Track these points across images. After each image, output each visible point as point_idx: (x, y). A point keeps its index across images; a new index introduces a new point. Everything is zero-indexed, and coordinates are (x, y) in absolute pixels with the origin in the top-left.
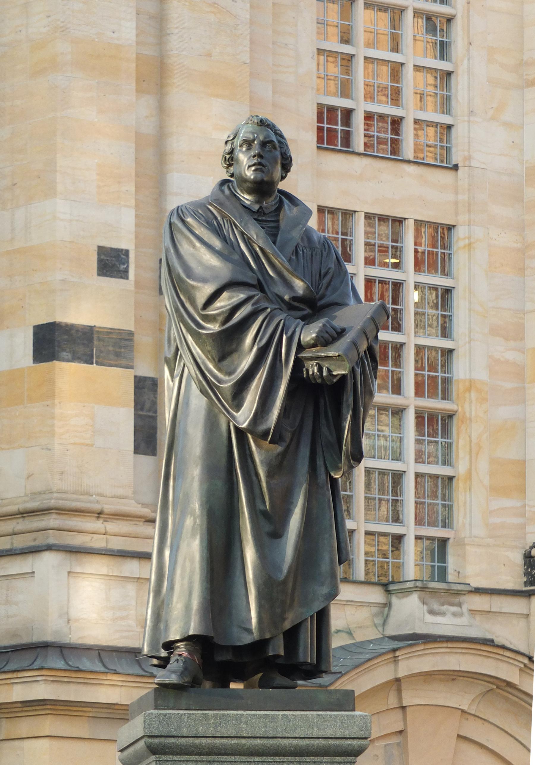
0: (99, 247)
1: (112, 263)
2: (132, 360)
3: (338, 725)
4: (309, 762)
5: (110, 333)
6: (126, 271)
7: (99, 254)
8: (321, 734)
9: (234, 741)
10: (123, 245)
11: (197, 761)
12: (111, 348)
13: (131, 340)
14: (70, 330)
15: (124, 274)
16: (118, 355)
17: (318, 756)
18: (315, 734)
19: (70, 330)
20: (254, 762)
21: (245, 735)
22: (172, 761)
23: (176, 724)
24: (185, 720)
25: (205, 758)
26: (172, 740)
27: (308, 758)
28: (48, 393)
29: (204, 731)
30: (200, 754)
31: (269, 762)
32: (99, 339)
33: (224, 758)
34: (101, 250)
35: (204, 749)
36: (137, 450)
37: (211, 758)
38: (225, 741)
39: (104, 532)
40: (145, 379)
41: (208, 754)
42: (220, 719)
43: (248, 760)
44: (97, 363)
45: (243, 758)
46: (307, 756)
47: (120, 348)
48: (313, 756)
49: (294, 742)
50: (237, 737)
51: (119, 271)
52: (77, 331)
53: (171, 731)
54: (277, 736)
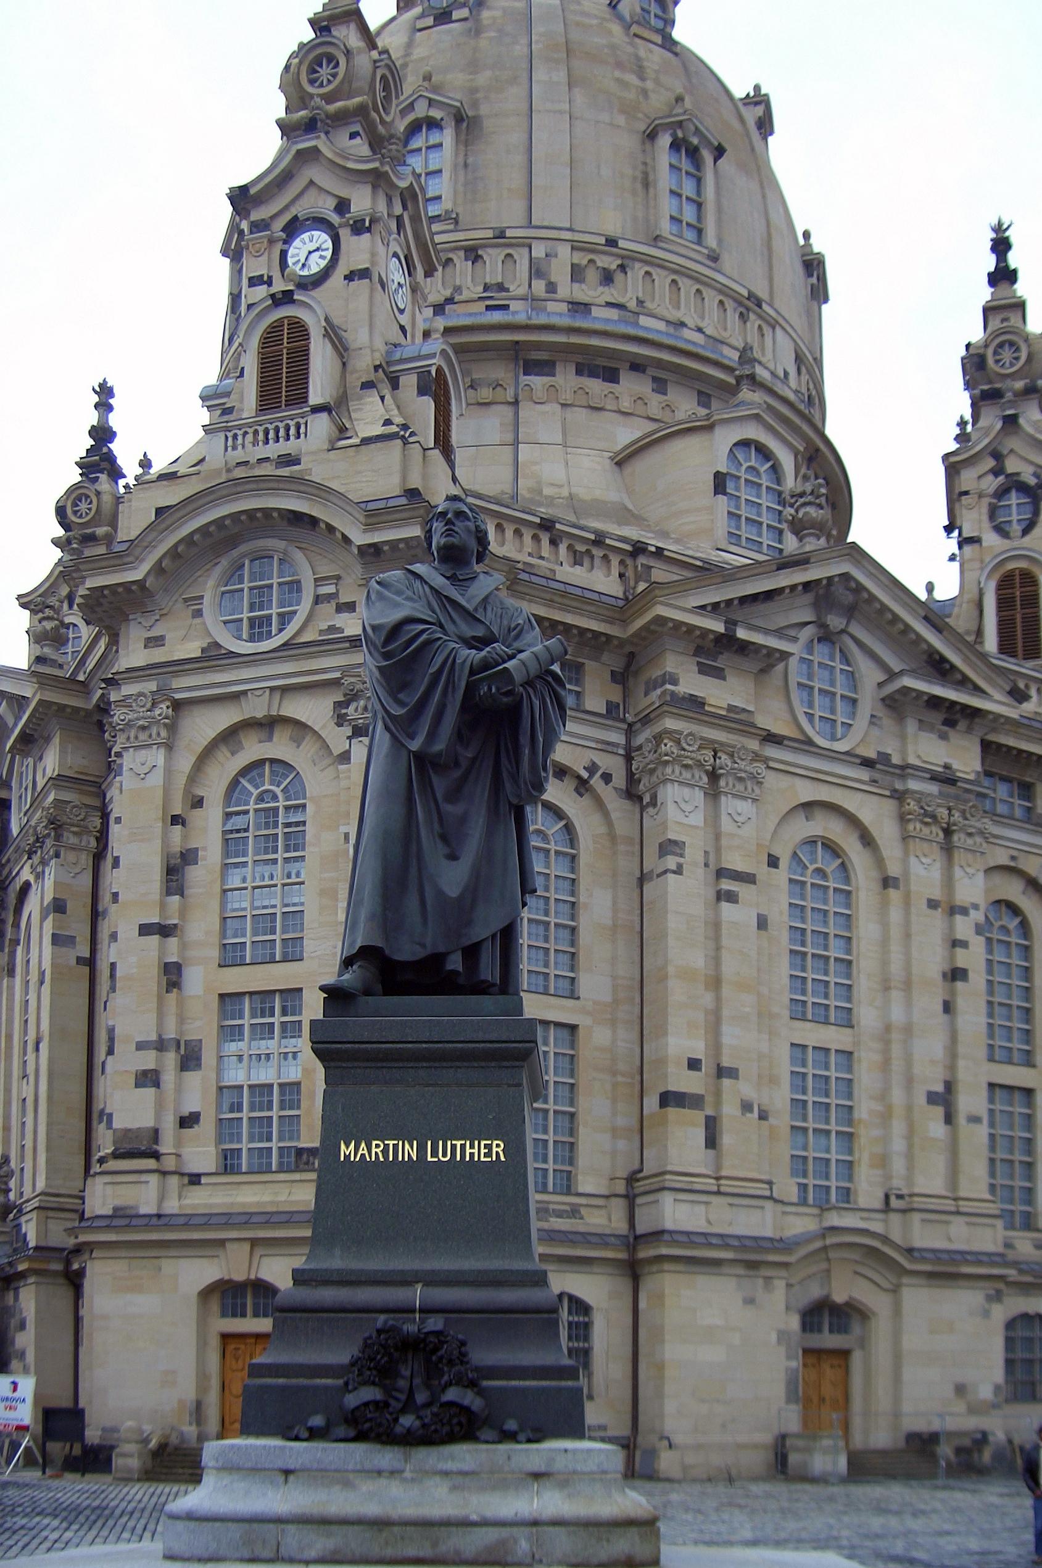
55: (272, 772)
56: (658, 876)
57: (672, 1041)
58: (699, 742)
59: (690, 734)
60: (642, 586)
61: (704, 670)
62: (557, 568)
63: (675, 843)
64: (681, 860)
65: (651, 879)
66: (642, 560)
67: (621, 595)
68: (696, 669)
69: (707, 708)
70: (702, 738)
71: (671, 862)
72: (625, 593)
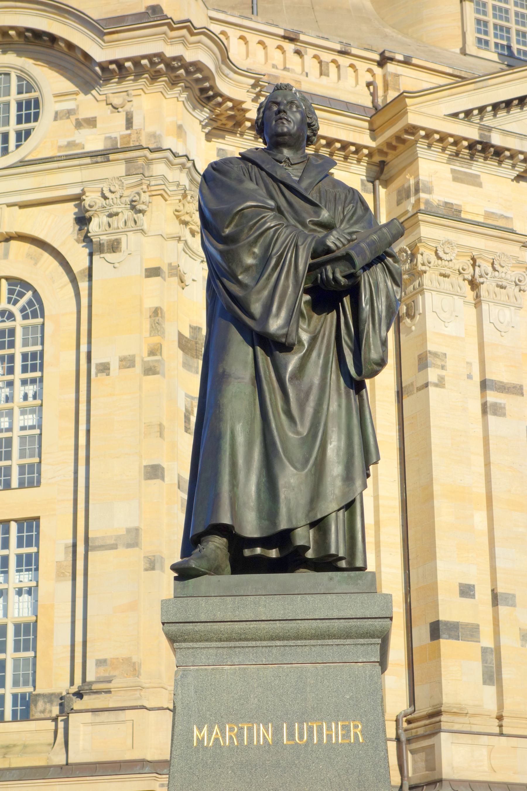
0: (460, 584)
1: (467, 591)
2: (479, 638)
3: (358, 605)
4: (332, 645)
5: (467, 625)
6: (474, 595)
7: (460, 587)
8: (341, 615)
9: (253, 625)
10: (472, 583)
11: (218, 648)
12: (468, 633)
13: (479, 629)
14: (447, 624)
15: (473, 596)
16: (472, 636)
17: (340, 638)
18: (335, 616)
19: (447, 624)
20: (276, 646)
21: (263, 619)
22: (193, 648)
23: (193, 610)
24: (203, 605)
25: (225, 644)
26: (190, 626)
27: (330, 641)
28: (436, 655)
29: (222, 616)
30: (220, 640)
31: (290, 646)
32: (462, 628)
33: (245, 644)
34: (461, 585)
35: (223, 634)
36: (485, 683)
37: (232, 644)
38: (243, 625)
39: (469, 722)
40: (487, 648)
41: (229, 639)
42: (238, 603)
43: (269, 645)
44: (462, 640)
45: (265, 643)
46: (329, 639)
47: (473, 632)
48: (335, 639)
49: (314, 624)
50: (256, 621)
51: (470, 595)
52: (451, 624)
53: (188, 617)
54: (296, 618)
55: (11, 292)
56: (419, 389)
57: (440, 564)
58: (456, 250)
59: (449, 242)
60: (392, 95)
61: (457, 177)
62: (303, 78)
63: (435, 355)
64: (443, 373)
65: (410, 393)
66: (391, 67)
67: (370, 105)
68: (450, 176)
69: (463, 215)
70: (459, 246)
71: (432, 374)
72: (373, 102)
